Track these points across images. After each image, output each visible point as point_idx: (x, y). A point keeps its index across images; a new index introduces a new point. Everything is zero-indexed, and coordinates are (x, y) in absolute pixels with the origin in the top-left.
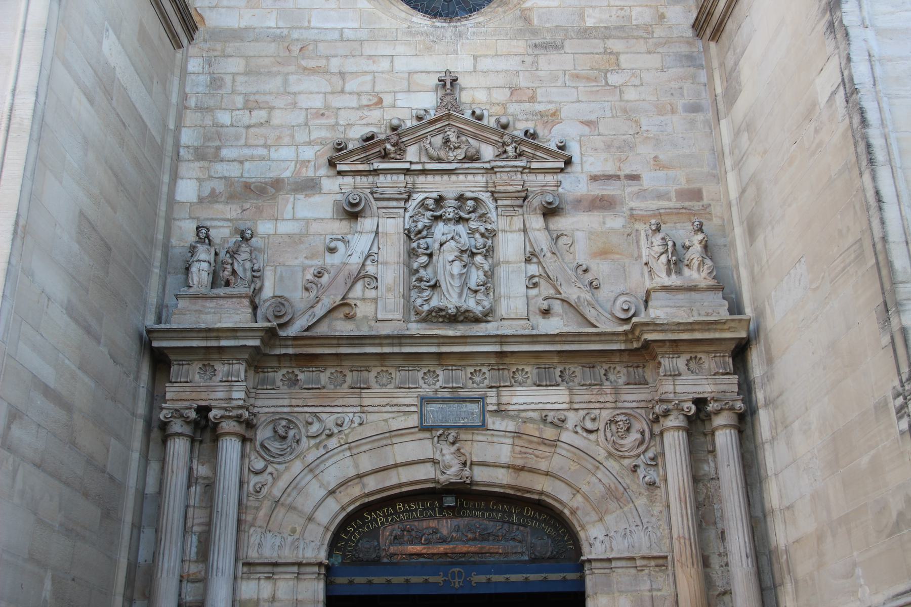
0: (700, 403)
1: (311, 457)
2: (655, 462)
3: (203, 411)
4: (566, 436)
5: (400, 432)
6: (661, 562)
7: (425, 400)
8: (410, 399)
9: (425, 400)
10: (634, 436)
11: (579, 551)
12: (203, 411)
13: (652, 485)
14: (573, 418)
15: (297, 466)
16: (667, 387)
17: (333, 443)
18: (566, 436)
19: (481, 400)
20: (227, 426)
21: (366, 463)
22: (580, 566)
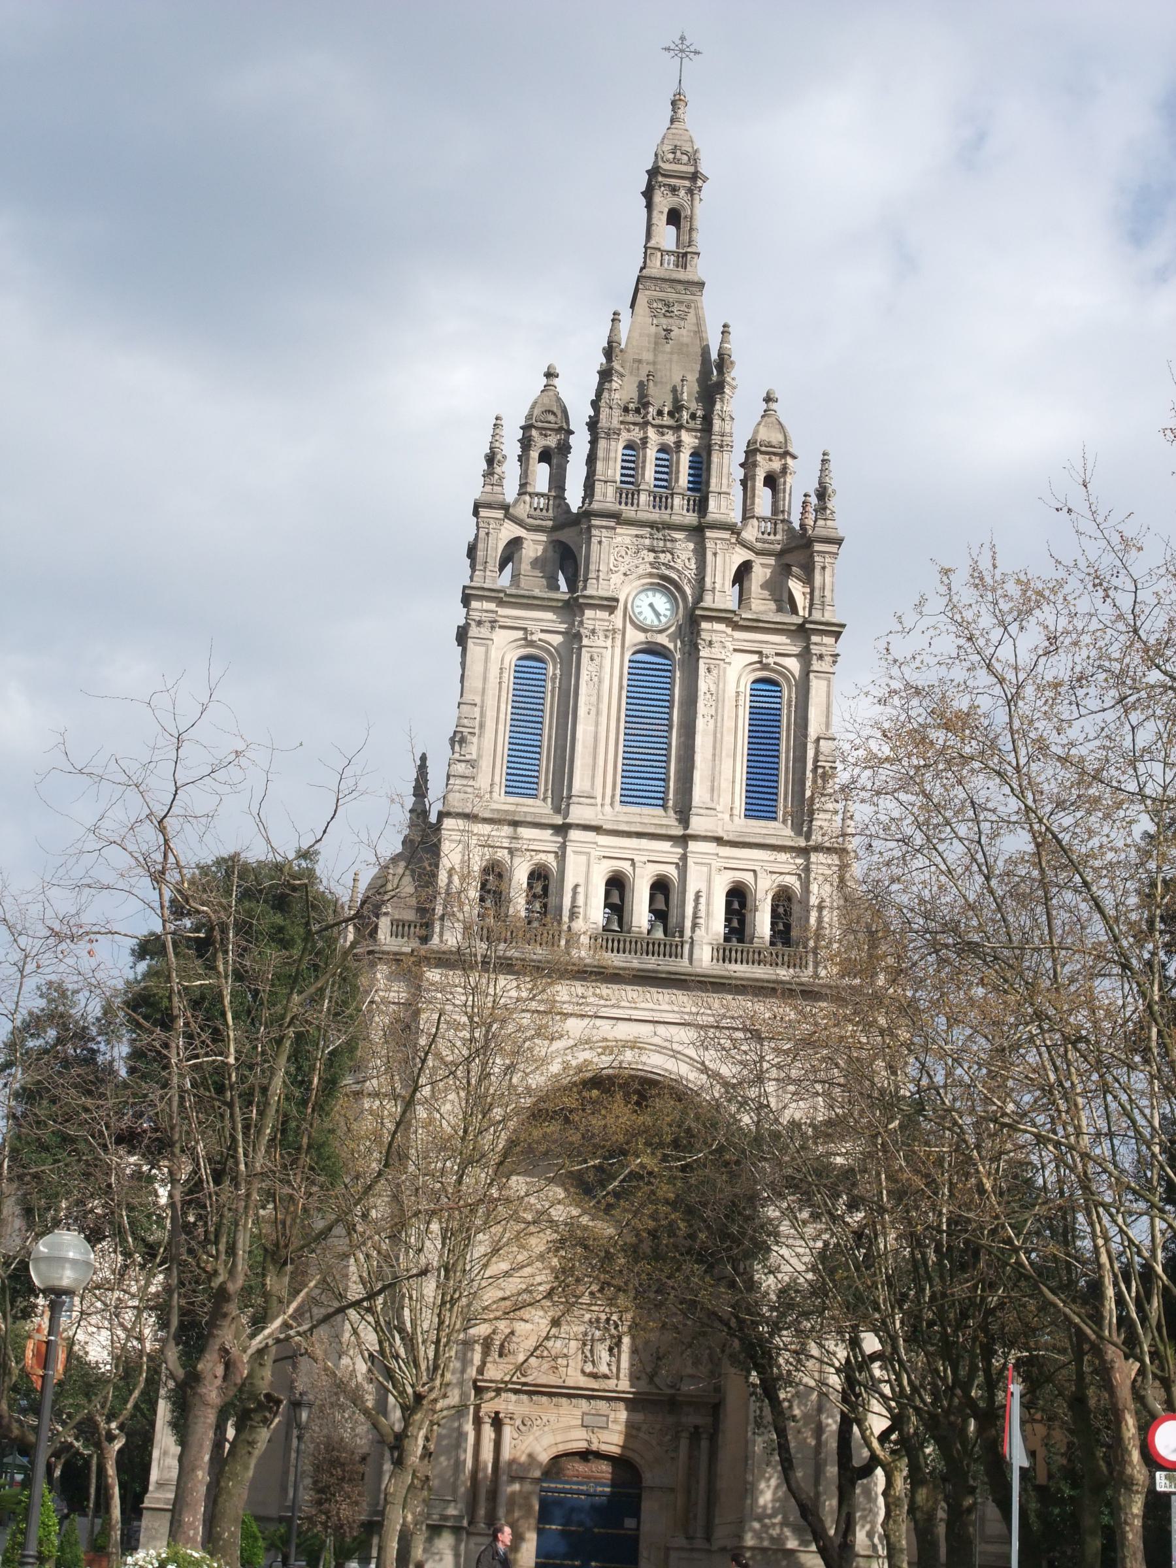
0: (696, 1427)
1: (538, 1434)
2: (676, 1450)
3: (497, 1413)
4: (641, 1435)
5: (575, 1427)
6: (672, 1490)
7: (584, 1414)
8: (578, 1413)
9: (584, 1414)
10: (669, 1437)
11: (641, 1482)
12: (497, 1413)
13: (673, 1458)
14: (644, 1427)
15: (531, 1438)
16: (684, 1420)
17: (546, 1429)
18: (641, 1435)
19: (607, 1416)
20: (507, 1421)
21: (559, 1439)
22: (640, 1488)
